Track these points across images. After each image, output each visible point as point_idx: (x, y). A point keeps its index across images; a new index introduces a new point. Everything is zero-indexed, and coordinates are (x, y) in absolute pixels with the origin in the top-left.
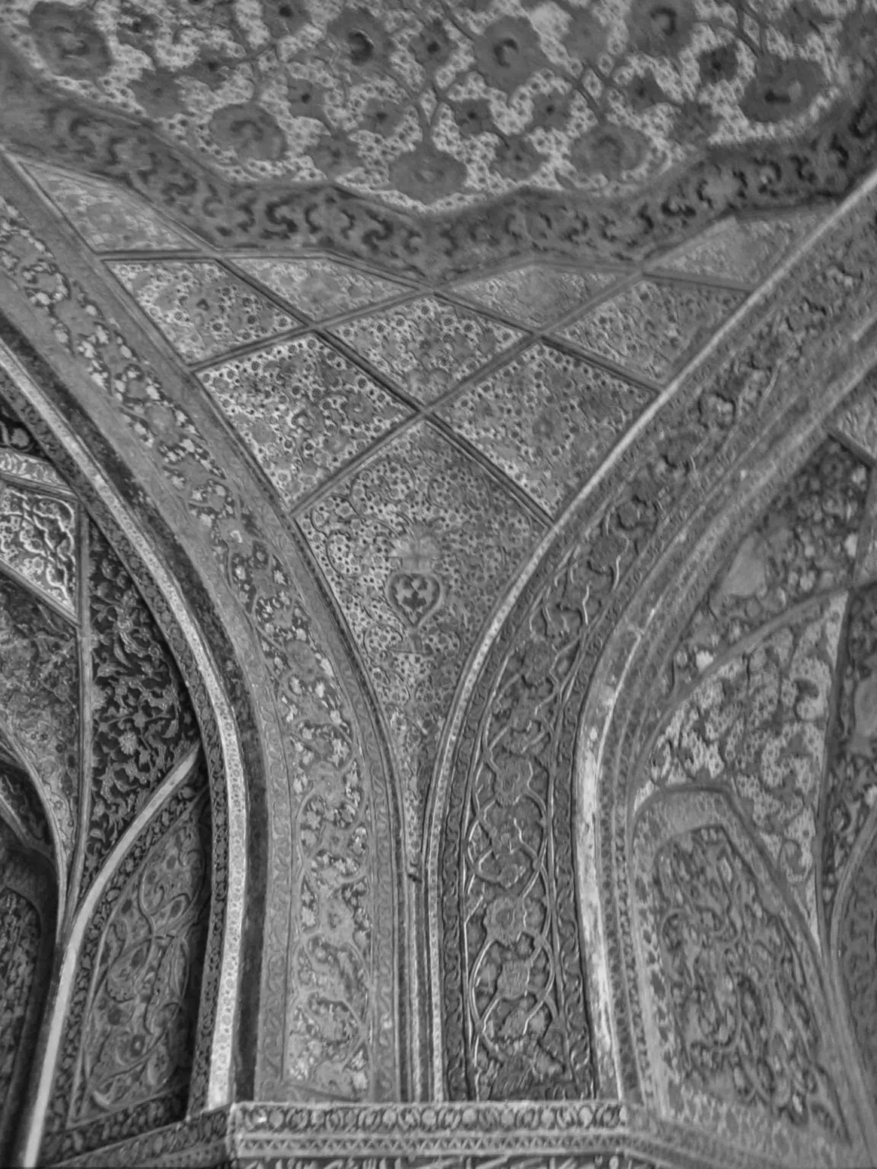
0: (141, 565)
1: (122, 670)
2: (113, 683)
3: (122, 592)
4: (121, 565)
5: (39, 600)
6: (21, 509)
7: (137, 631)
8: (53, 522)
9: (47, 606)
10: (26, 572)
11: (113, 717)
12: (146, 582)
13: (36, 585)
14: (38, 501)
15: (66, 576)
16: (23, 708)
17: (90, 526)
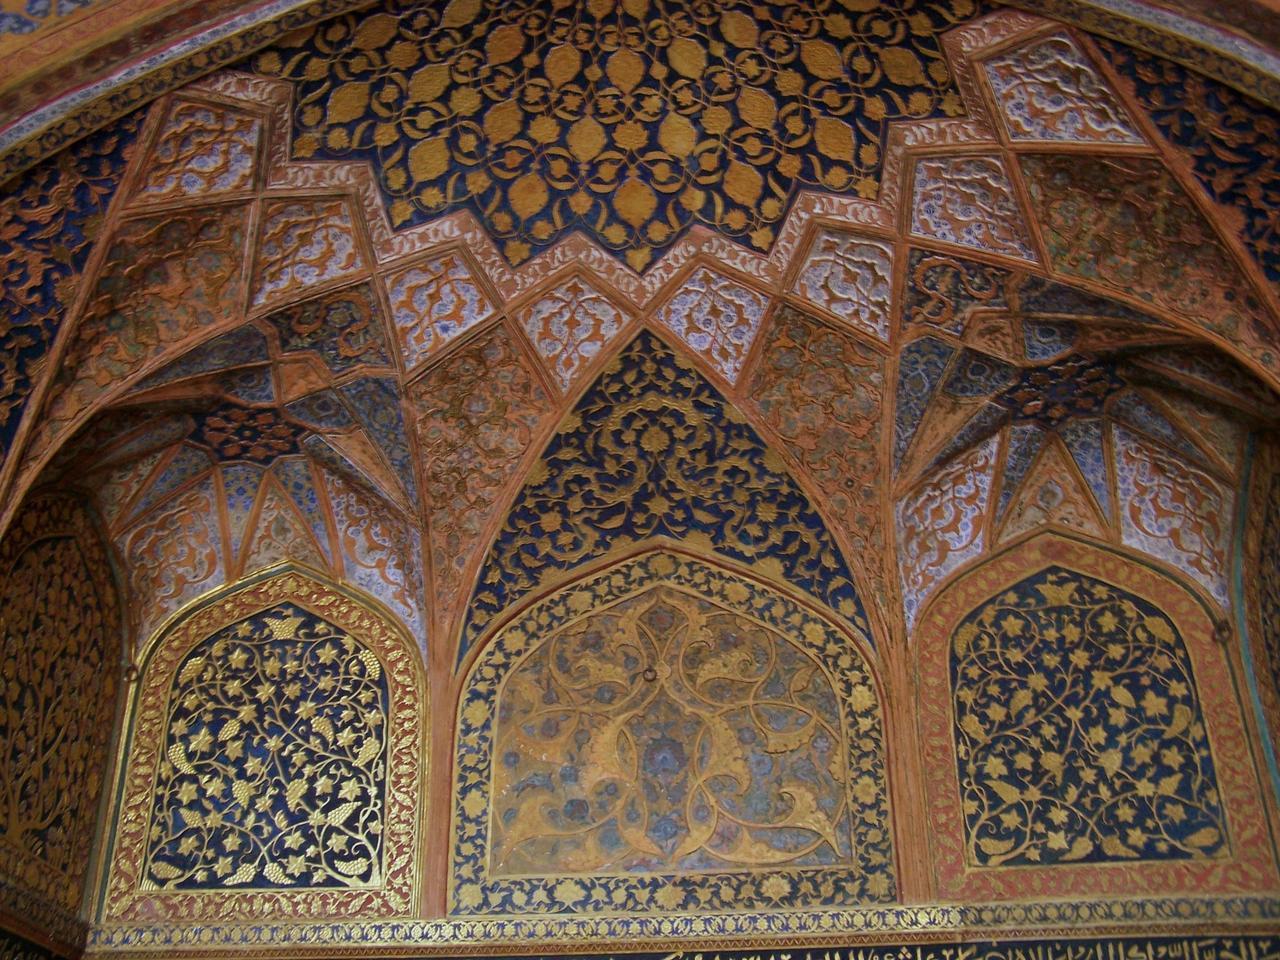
0: (1179, 42)
1: (1240, 171)
2: (1240, 191)
3: (1180, 86)
4: (1156, 58)
5: (1100, 156)
6: (1016, 76)
7: (1228, 117)
8: (1057, 66)
9: (1108, 155)
10: (1066, 136)
11: (1265, 228)
12: (1200, 57)
13: (1085, 142)
14: (1025, 56)
15: (1110, 112)
16: (1162, 277)
17: (1098, 44)
